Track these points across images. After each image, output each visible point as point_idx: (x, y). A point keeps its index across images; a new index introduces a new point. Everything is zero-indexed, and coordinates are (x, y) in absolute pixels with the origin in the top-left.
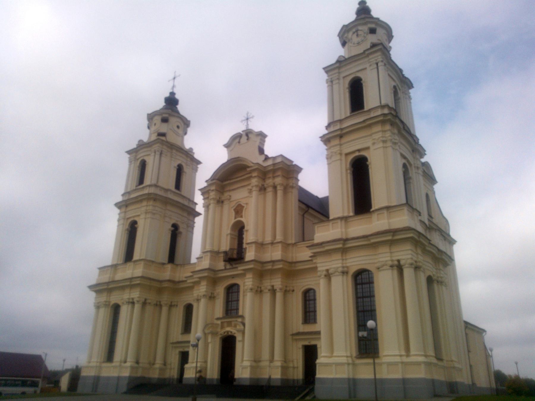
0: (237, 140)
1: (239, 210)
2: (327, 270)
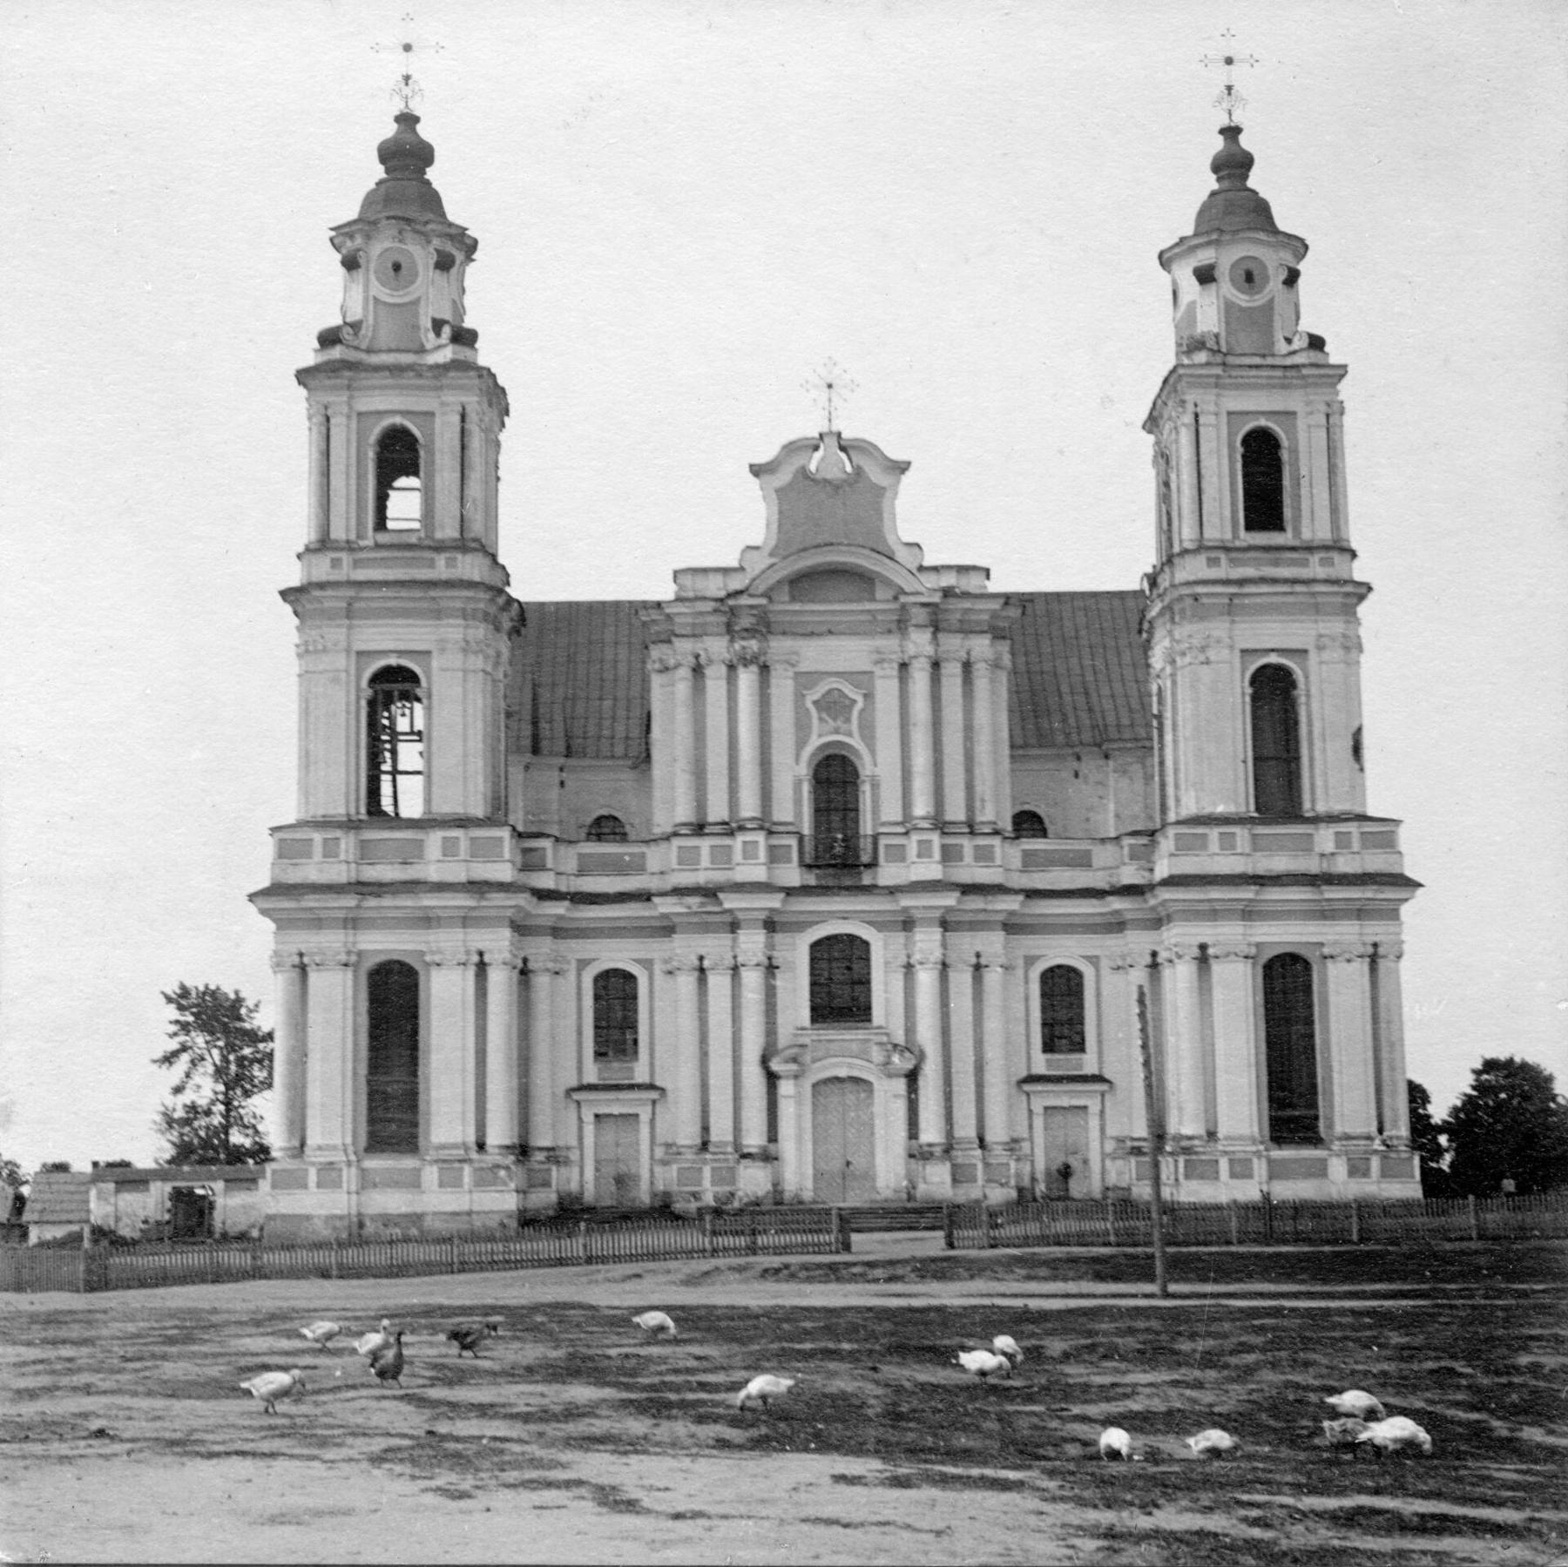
2: (1203, 947)
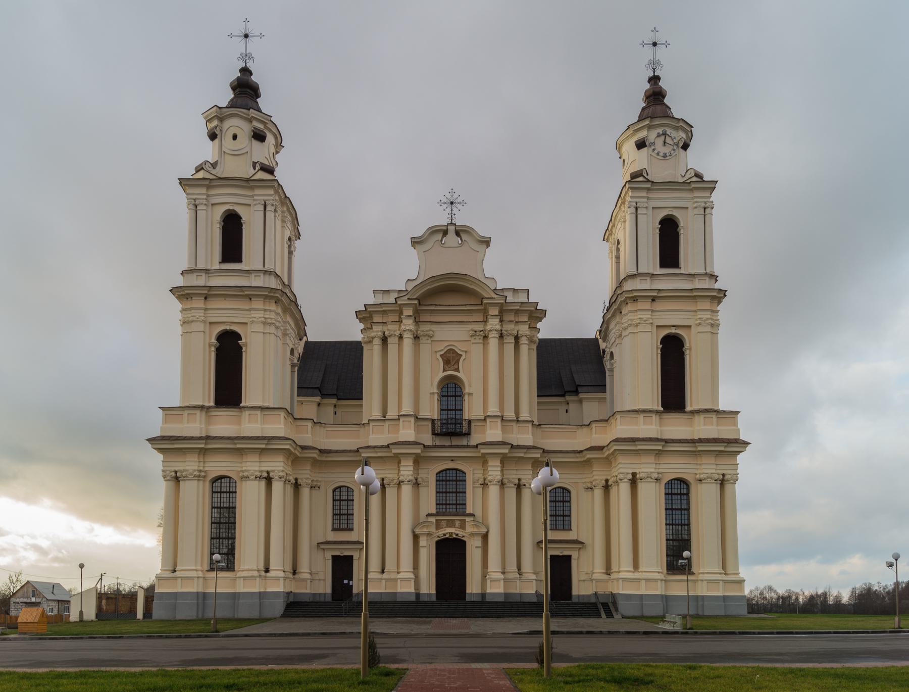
0: (439, 236)
1: (451, 358)
2: (634, 474)
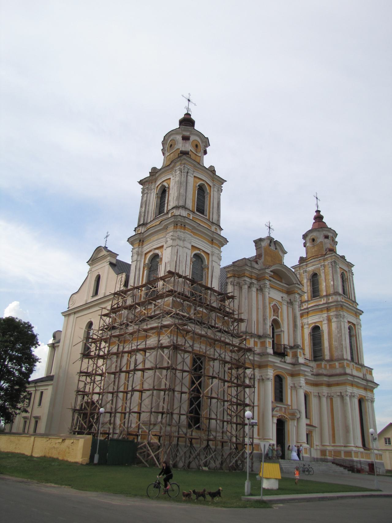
1: (276, 310)
2: (351, 393)
